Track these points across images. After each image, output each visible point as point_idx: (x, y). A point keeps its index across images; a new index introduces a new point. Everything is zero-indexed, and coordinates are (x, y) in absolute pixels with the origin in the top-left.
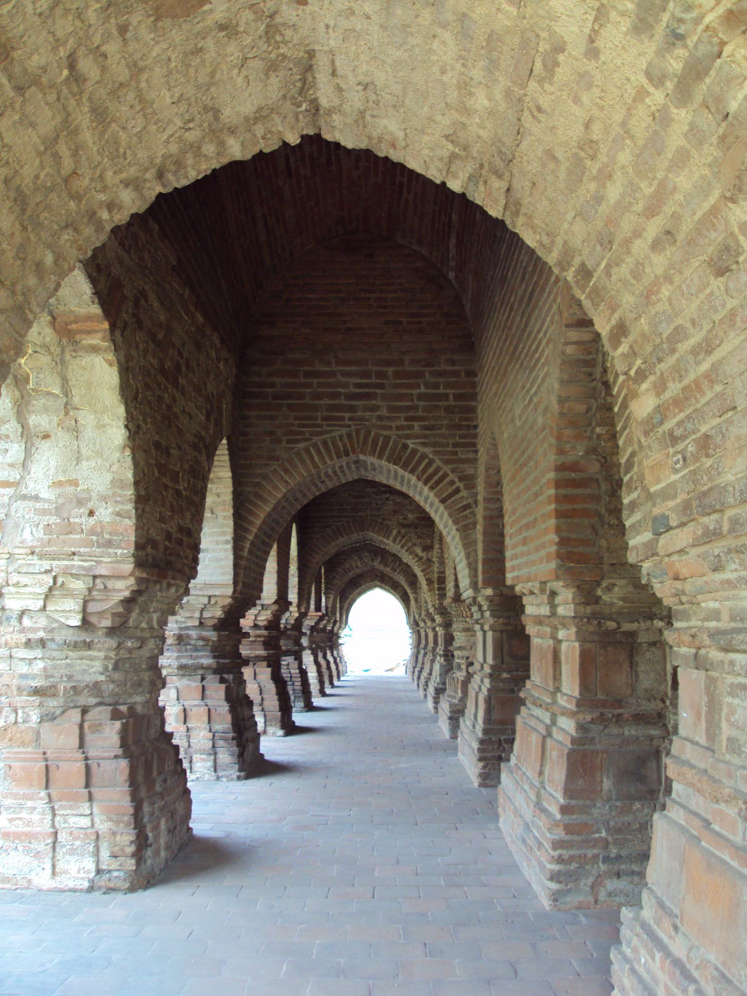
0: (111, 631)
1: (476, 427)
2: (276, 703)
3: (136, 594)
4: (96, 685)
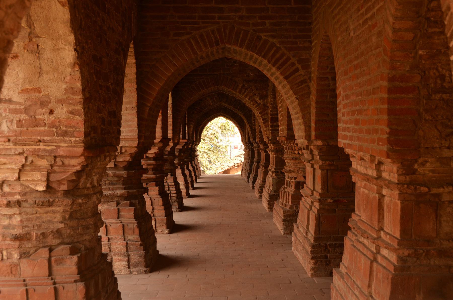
0: (66, 193)
1: (310, 23)
2: (163, 212)
3: (84, 167)
4: (59, 232)
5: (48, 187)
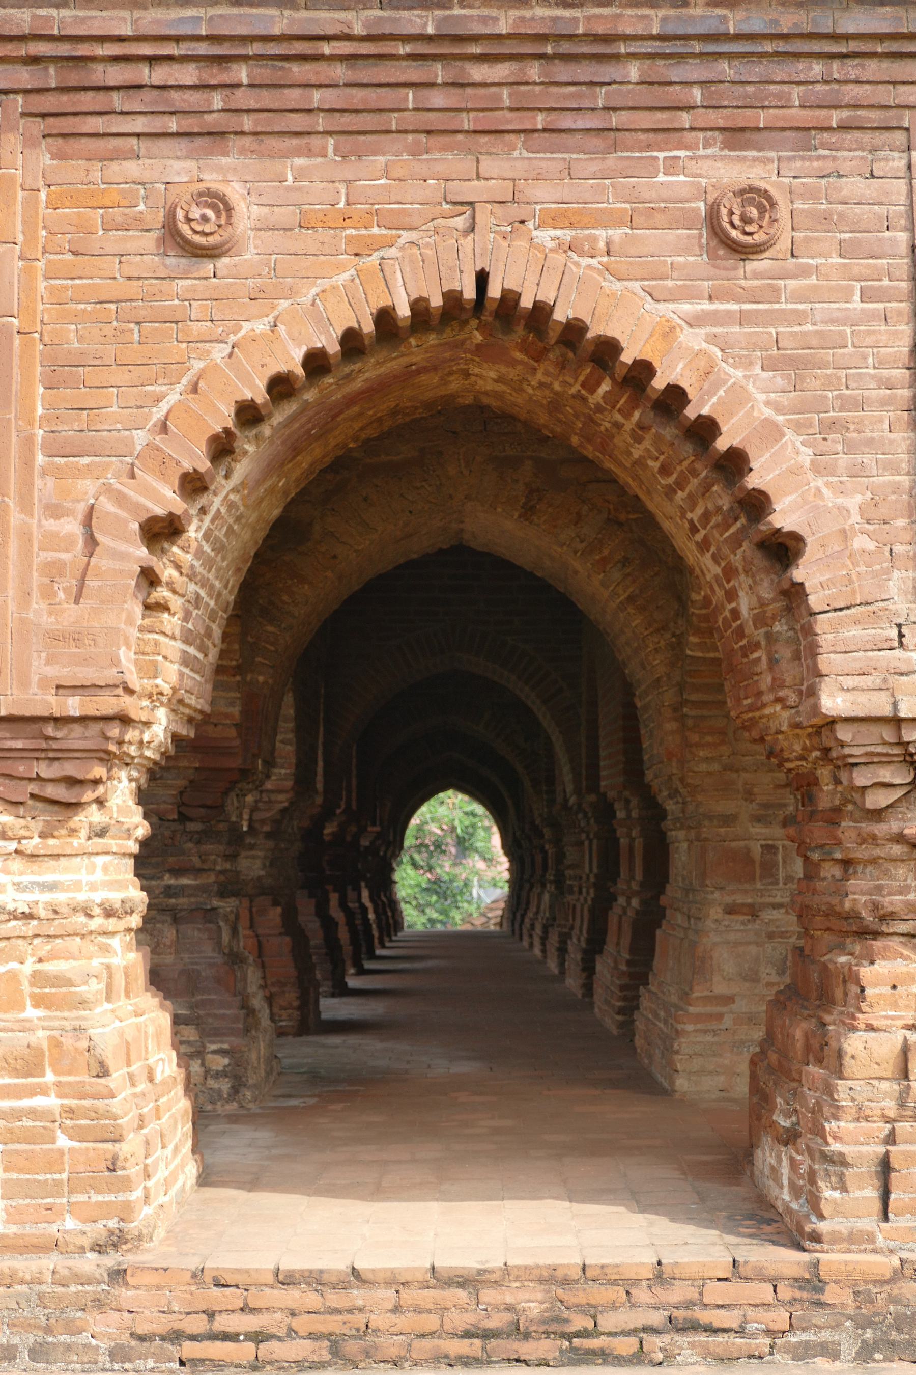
0: (269, 835)
3: (292, 803)
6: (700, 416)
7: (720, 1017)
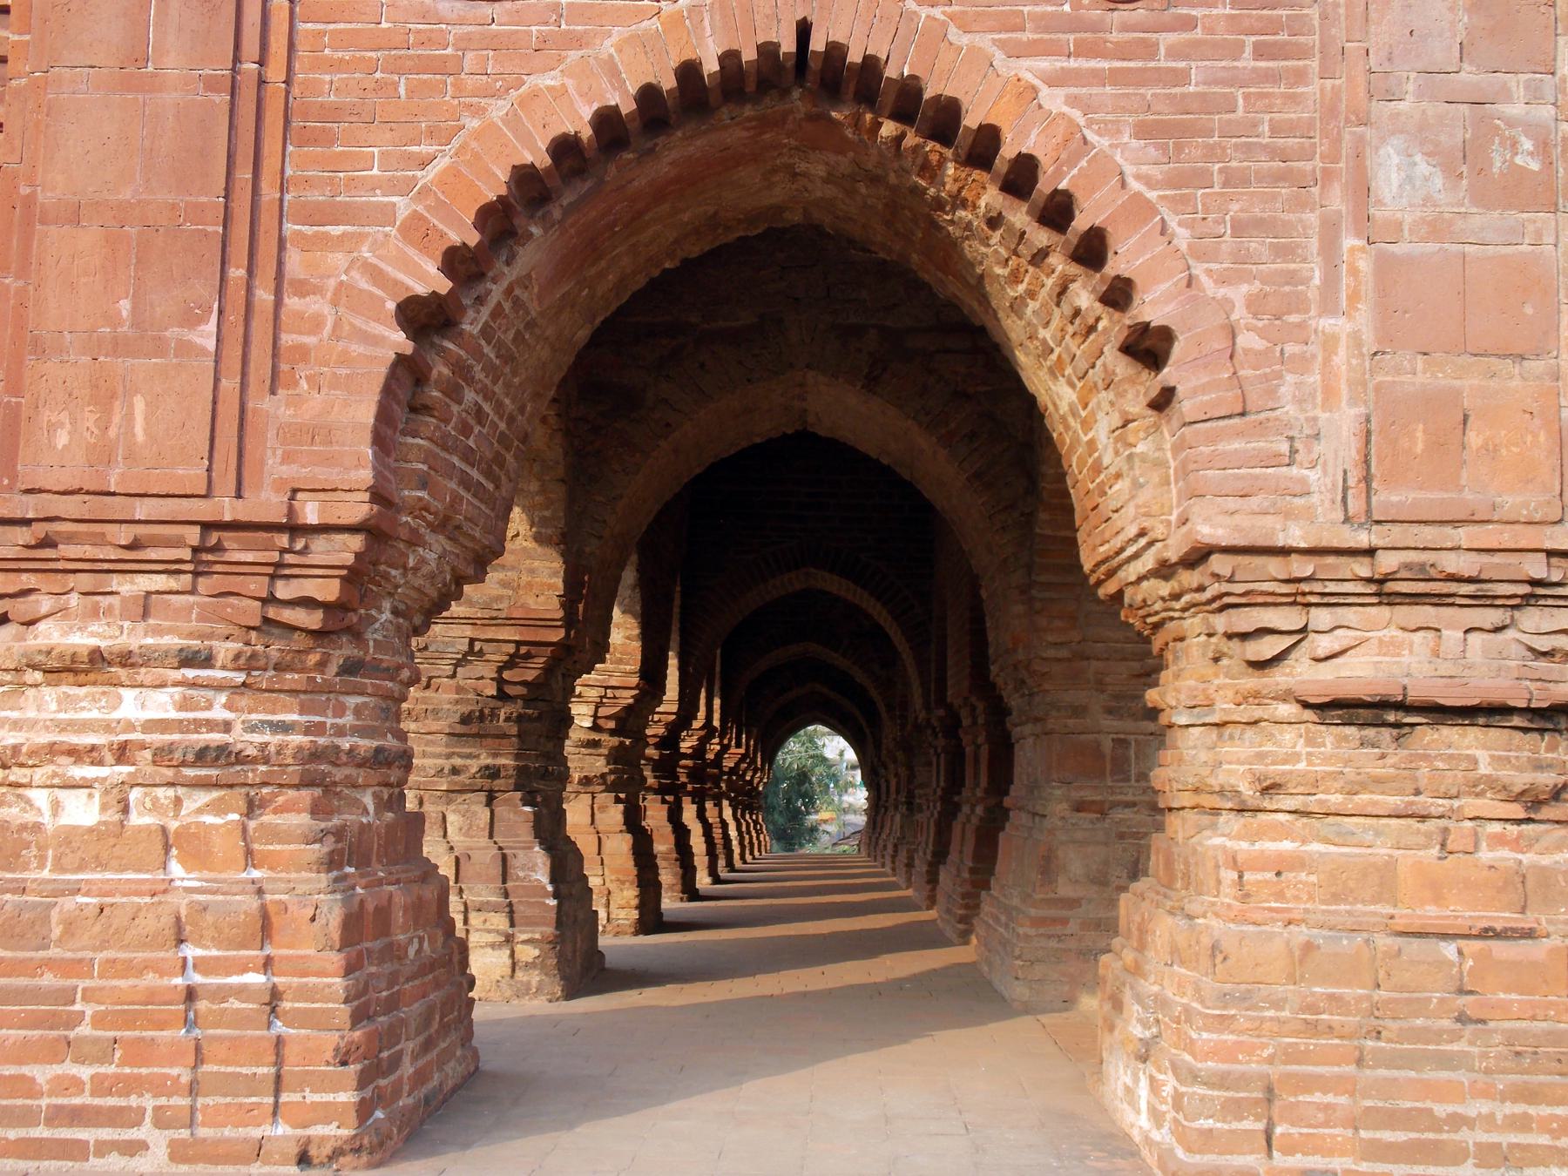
4: (603, 776)
5: (594, 722)
6: (1056, 190)
7: (1064, 922)
